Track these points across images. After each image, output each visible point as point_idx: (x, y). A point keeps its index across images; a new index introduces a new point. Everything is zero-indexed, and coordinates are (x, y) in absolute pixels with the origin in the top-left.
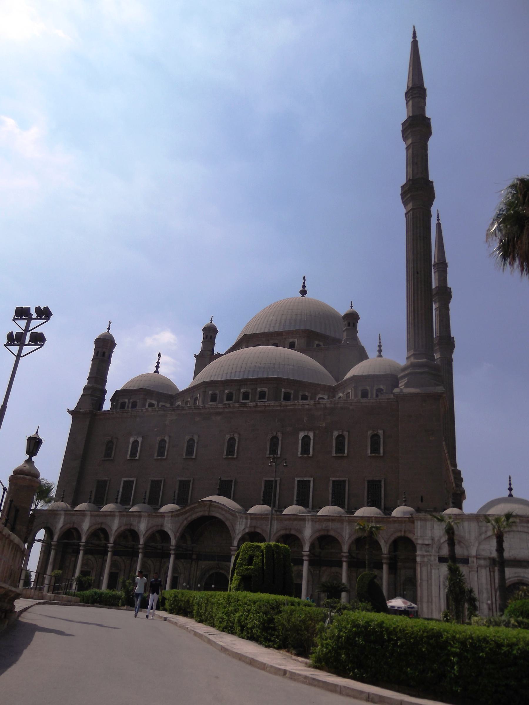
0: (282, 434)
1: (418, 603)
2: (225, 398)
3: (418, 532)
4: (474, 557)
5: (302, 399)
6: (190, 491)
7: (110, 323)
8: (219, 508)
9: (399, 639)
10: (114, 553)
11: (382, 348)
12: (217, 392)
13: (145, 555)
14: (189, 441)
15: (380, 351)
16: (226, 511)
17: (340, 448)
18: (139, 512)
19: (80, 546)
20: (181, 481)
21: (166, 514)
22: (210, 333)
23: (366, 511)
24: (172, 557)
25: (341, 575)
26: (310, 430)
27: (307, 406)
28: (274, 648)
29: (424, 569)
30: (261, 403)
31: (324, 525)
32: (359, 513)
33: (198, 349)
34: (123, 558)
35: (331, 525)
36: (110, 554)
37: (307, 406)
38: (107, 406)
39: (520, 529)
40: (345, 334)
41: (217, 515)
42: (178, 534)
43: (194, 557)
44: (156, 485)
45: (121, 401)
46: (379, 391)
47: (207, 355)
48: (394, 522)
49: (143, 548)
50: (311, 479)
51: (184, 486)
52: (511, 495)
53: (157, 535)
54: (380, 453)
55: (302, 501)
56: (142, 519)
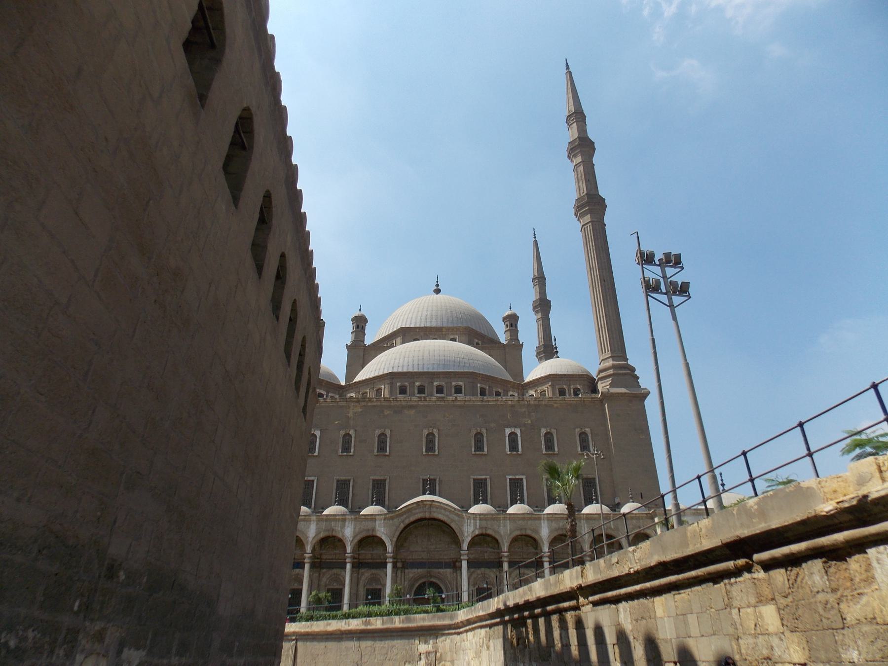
2: (416, 391)
6: (387, 491)
8: (442, 508)
14: (379, 436)
16: (450, 511)
17: (549, 446)
20: (374, 480)
21: (377, 517)
22: (360, 323)
26: (515, 427)
27: (510, 403)
30: (460, 397)
33: (349, 339)
37: (510, 403)
41: (440, 517)
42: (395, 539)
49: (351, 557)
50: (524, 477)
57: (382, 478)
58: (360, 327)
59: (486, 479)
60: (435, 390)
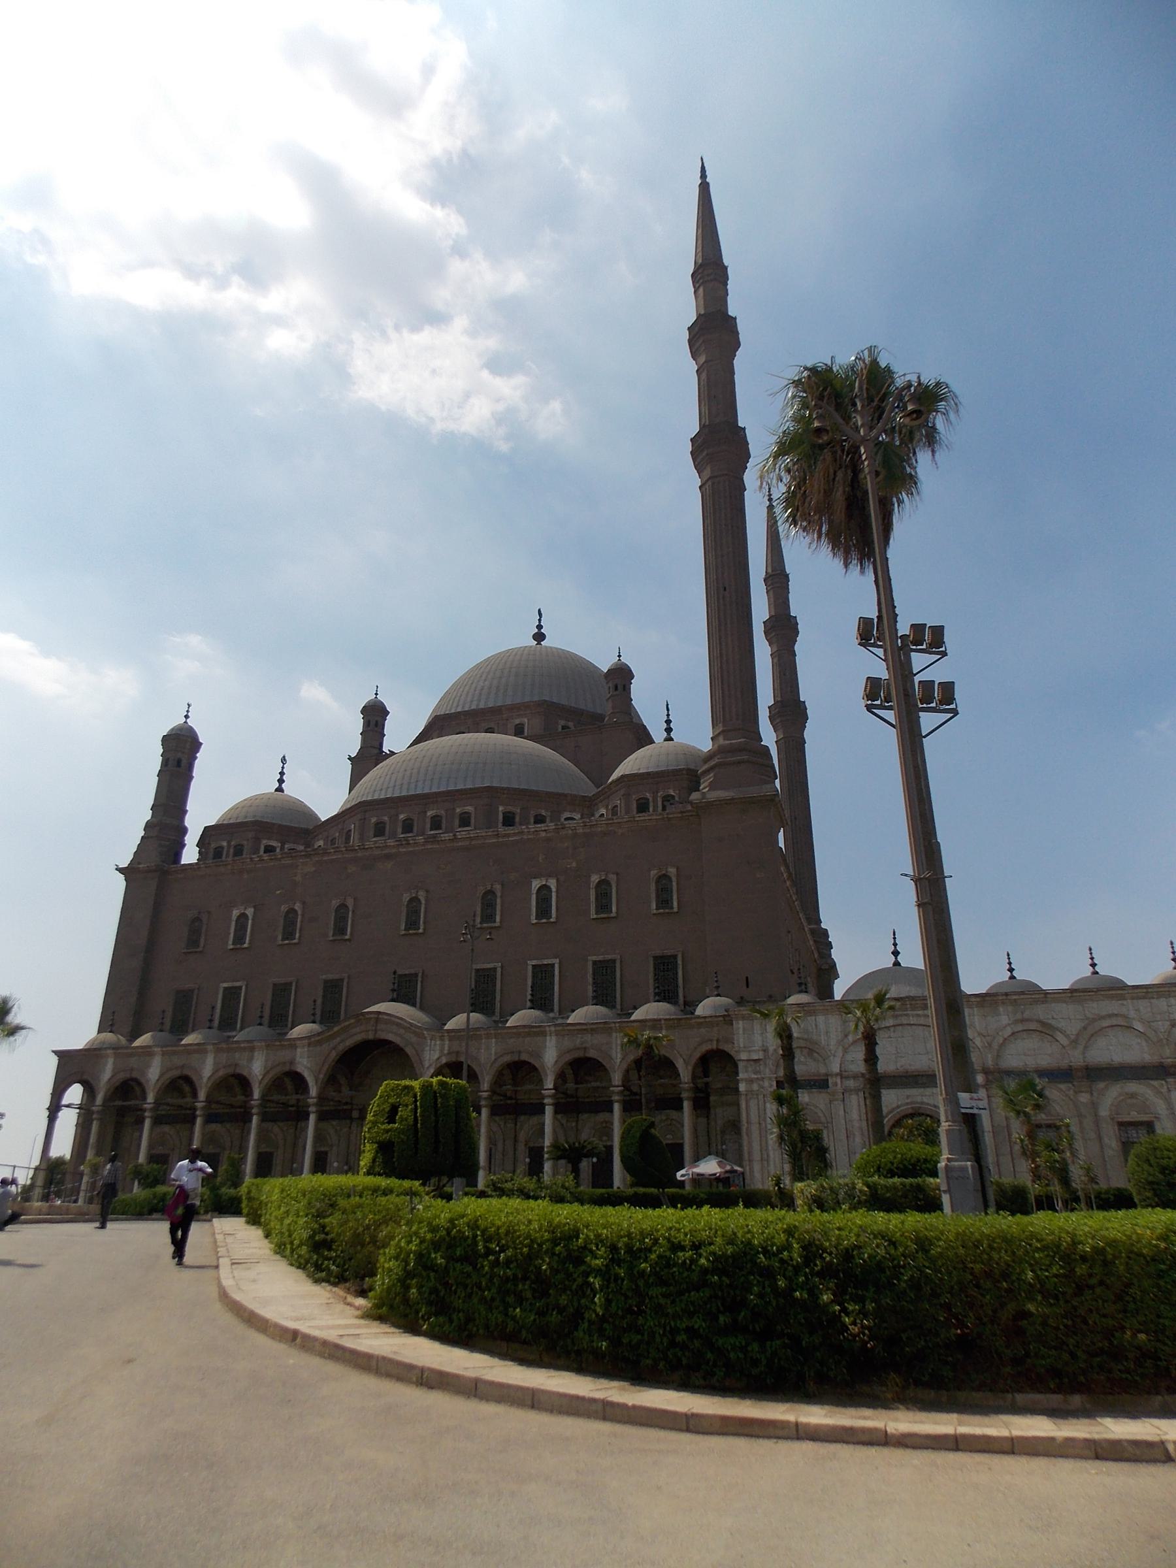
0: (502, 885)
1: (746, 1163)
2: (400, 830)
3: (740, 1040)
4: (837, 1075)
6: (344, 999)
7: (189, 705)
9: (502, 1250)
11: (672, 725)
12: (386, 818)
13: (265, 1118)
15: (669, 730)
16: (405, 1028)
17: (603, 904)
18: (248, 1042)
19: (144, 1110)
20: (326, 982)
21: (298, 1042)
22: (374, 716)
23: (650, 1010)
24: (312, 1118)
25: (612, 1124)
26: (550, 876)
28: (328, 1281)
29: (753, 1103)
30: (462, 833)
32: (637, 1015)
33: (354, 746)
34: (228, 1125)
36: (199, 1121)
37: (543, 834)
38: (190, 855)
39: (913, 1020)
40: (610, 704)
41: (390, 1037)
42: (321, 1076)
44: (281, 991)
45: (213, 845)
46: (667, 799)
48: (700, 1025)
51: (333, 988)
52: (897, 964)
53: (286, 1080)
54: (672, 908)
55: (541, 1001)
56: (256, 1054)
57: (337, 977)
59: (495, 969)
60: (428, 826)
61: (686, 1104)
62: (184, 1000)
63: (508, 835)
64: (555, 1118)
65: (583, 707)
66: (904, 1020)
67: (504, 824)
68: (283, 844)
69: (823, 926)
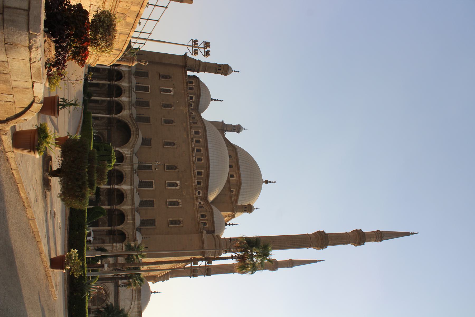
2: (196, 139)
5: (198, 182)
10: (109, 85)
13: (109, 102)
15: (230, 225)
20: (149, 117)
24: (108, 116)
26: (181, 187)
30: (195, 159)
31: (129, 196)
33: (227, 122)
35: (129, 199)
36: (109, 82)
38: (190, 73)
43: (109, 128)
44: (147, 104)
45: (193, 81)
46: (205, 224)
47: (222, 127)
48: (133, 232)
49: (113, 100)
51: (147, 120)
52: (152, 292)
55: (142, 184)
58: (235, 128)
59: (152, 170)
61: (110, 228)
62: (145, 74)
63: (194, 173)
64: (106, 188)
65: (240, 197)
66: (134, 292)
67: (198, 172)
68: (194, 102)
69: (170, 279)
